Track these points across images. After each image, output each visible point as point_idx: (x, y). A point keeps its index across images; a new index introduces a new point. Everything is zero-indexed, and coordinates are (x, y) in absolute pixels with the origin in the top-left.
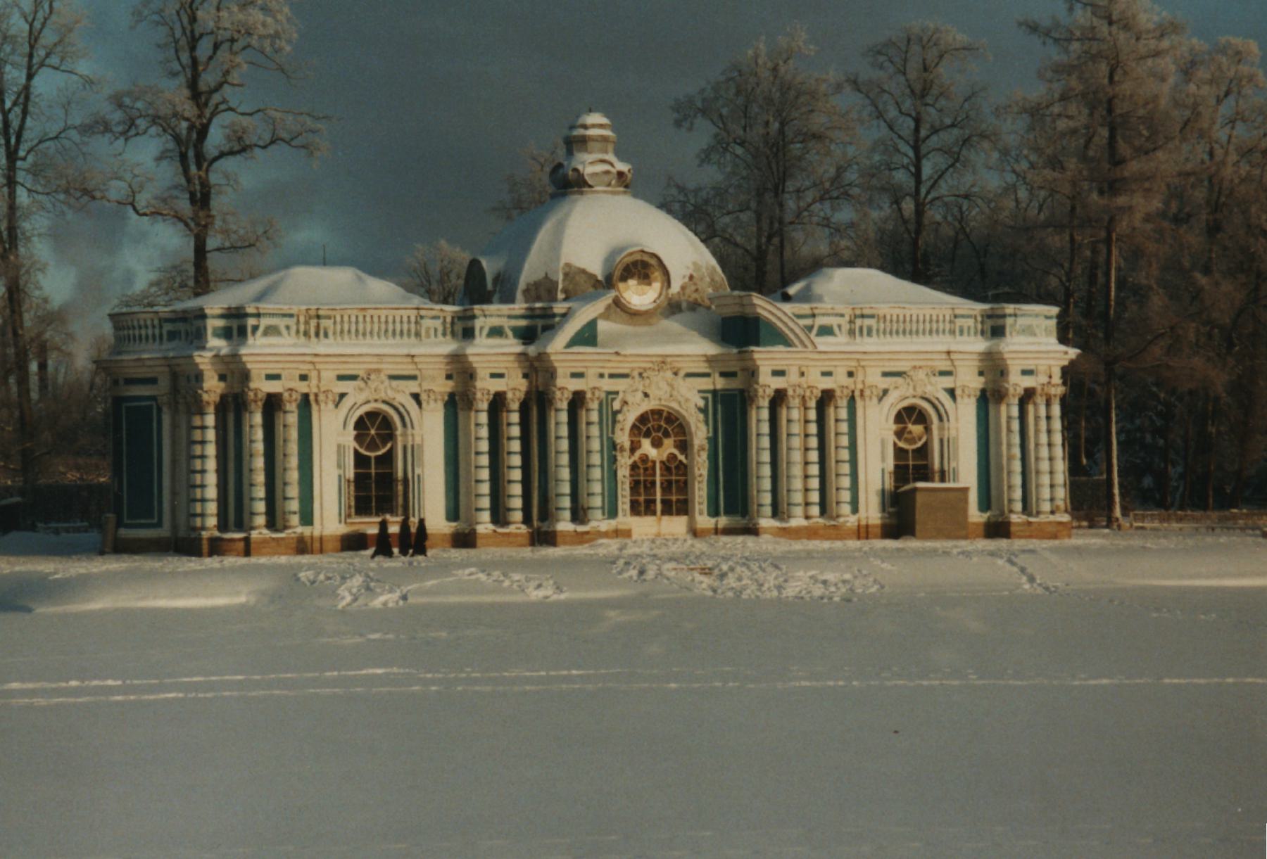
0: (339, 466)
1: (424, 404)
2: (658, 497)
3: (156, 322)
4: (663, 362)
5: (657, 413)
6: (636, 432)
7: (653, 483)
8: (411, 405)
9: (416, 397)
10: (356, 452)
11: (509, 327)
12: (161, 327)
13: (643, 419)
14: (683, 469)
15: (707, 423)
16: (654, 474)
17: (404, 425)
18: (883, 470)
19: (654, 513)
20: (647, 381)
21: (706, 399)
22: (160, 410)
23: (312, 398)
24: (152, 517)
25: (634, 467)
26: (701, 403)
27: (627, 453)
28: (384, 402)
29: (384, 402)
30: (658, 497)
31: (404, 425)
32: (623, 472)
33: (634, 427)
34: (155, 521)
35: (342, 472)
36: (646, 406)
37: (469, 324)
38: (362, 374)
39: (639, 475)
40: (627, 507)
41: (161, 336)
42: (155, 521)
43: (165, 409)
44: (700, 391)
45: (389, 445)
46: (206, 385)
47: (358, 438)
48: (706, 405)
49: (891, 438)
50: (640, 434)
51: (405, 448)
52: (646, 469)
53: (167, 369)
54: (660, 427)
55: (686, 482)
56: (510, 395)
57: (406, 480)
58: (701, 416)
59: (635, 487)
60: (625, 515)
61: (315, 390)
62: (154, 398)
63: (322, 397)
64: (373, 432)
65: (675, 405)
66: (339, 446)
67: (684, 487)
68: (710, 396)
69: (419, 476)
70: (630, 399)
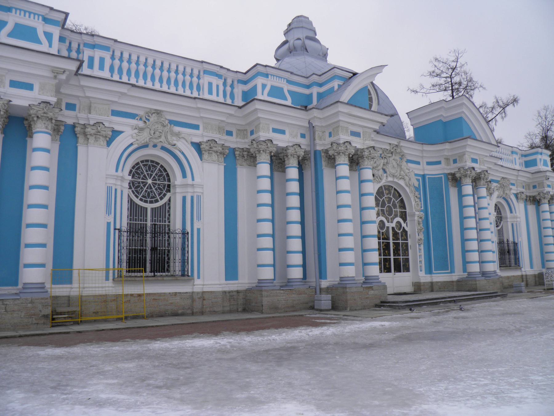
0: (108, 212)
1: (206, 156)
2: (392, 257)
9: (197, 146)
10: (131, 202)
11: (290, 92)
15: (420, 198)
19: (389, 270)
20: (386, 161)
21: (418, 180)
23: (78, 129)
26: (416, 184)
29: (163, 148)
30: (392, 257)
31: (184, 176)
38: (141, 113)
45: (165, 200)
48: (419, 185)
51: (184, 199)
56: (291, 151)
57: (184, 234)
58: (417, 193)
60: (421, 271)
64: (150, 181)
65: (402, 183)
66: (109, 189)
68: (420, 178)
69: (199, 230)
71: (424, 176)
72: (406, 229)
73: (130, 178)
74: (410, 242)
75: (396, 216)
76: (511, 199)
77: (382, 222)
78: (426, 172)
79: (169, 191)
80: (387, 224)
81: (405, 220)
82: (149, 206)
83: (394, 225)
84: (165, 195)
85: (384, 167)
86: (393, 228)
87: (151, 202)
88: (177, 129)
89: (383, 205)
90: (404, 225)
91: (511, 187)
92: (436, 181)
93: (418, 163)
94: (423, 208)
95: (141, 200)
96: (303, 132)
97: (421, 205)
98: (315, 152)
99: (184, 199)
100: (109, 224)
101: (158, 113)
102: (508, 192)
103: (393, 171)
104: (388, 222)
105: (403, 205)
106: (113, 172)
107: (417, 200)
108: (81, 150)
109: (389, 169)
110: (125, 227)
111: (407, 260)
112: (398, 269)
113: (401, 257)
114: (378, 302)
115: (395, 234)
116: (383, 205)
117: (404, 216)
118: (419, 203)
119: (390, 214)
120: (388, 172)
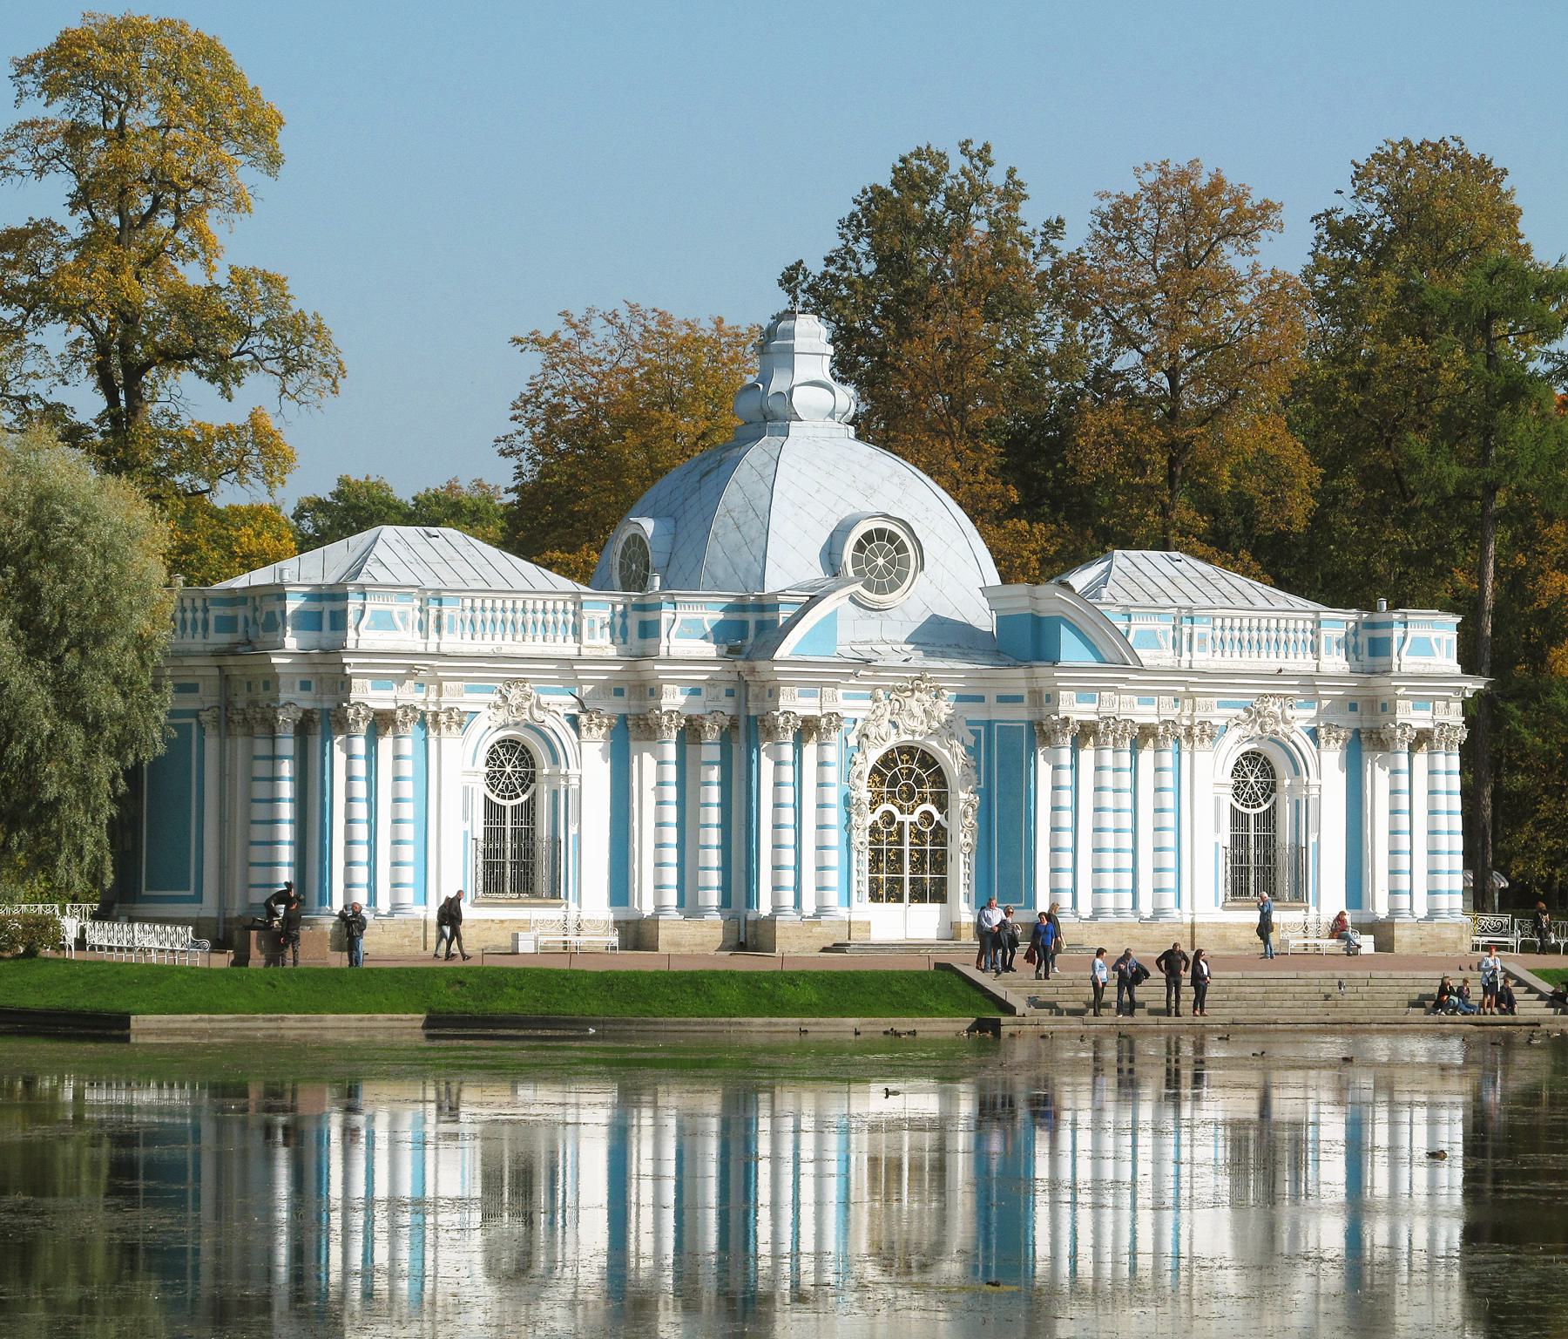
0: (466, 819)
2: (907, 876)
3: (199, 603)
4: (920, 679)
5: (908, 751)
6: (877, 779)
7: (900, 854)
8: (566, 734)
12: (206, 610)
13: (887, 761)
14: (940, 834)
16: (901, 843)
17: (556, 761)
18: (1217, 844)
19: (900, 899)
21: (976, 733)
22: (202, 730)
23: (429, 718)
24: (188, 889)
25: (874, 830)
26: (971, 740)
27: (865, 808)
28: (528, 726)
30: (907, 876)
32: (862, 837)
33: (875, 770)
34: (191, 892)
35: (468, 828)
36: (892, 741)
37: (649, 616)
39: (879, 842)
40: (866, 889)
41: (206, 623)
42: (191, 892)
43: (209, 730)
44: (969, 723)
46: (284, 696)
47: (492, 779)
48: (977, 742)
49: (1228, 799)
50: (882, 783)
52: (890, 834)
53: (216, 672)
54: (911, 771)
55: (944, 854)
57: (555, 841)
59: (875, 863)
61: (433, 708)
62: (196, 714)
63: (443, 718)
64: (508, 769)
66: (466, 789)
67: (940, 862)
68: (982, 729)
70: (872, 731)
71: (989, 724)
72: (943, 823)
73: (487, 770)
74: (951, 848)
75: (923, 800)
76: (1293, 742)
77: (890, 813)
78: (994, 717)
79: (532, 781)
80: (899, 817)
81: (942, 807)
82: (508, 804)
83: (915, 817)
84: (528, 787)
85: (894, 718)
86: (911, 824)
87: (511, 798)
88: (544, 699)
89: (894, 781)
90: (937, 816)
91: (1289, 713)
92: (1008, 731)
93: (981, 699)
94: (982, 786)
95: (498, 795)
96: (730, 686)
97: (979, 780)
98: (748, 717)
99: (555, 794)
100: (466, 833)
101: (525, 680)
102: (1281, 727)
103: (913, 724)
104: (902, 812)
105: (939, 778)
106: (468, 766)
107: (972, 772)
108: (433, 743)
109: (905, 721)
110: (481, 837)
111: (943, 882)
112: (919, 896)
113: (928, 876)
114: (829, 944)
115: (919, 835)
116: (894, 781)
117: (942, 806)
118: (974, 777)
119: (910, 797)
120: (901, 726)
